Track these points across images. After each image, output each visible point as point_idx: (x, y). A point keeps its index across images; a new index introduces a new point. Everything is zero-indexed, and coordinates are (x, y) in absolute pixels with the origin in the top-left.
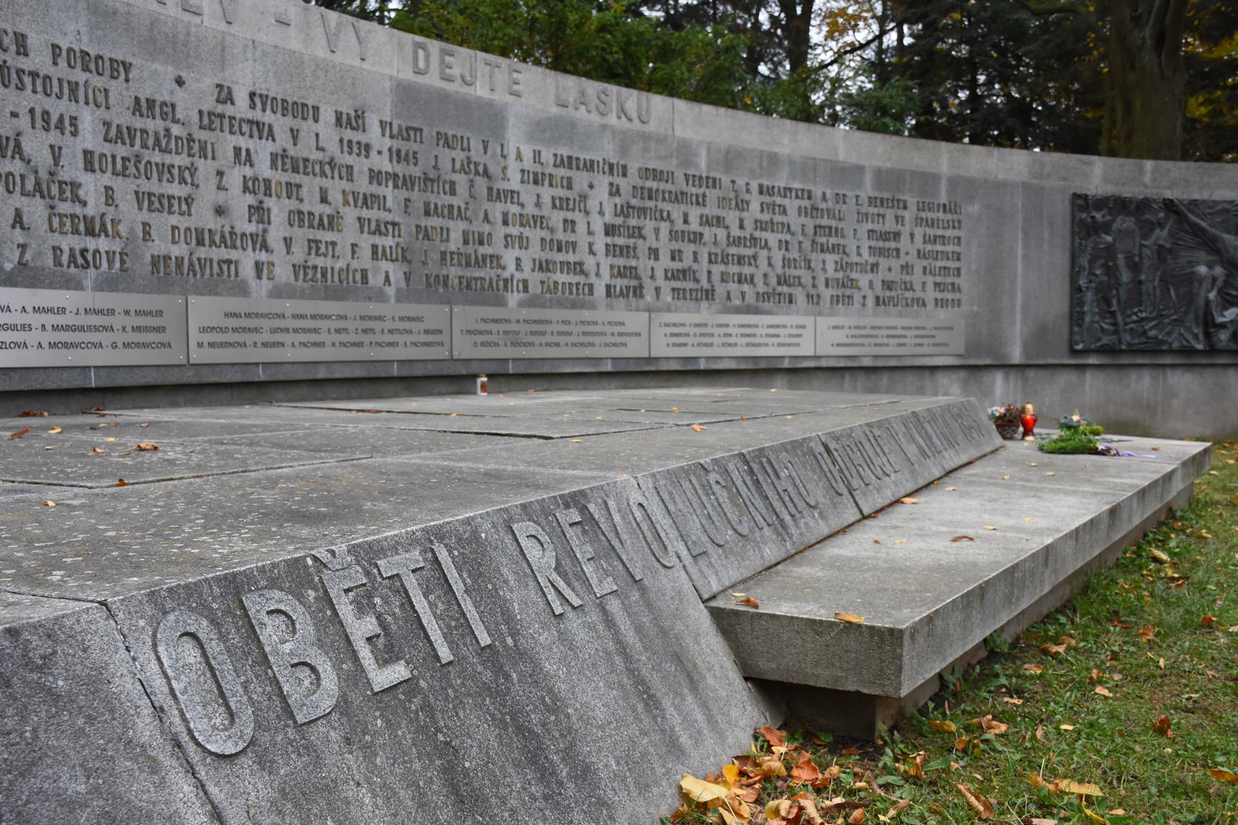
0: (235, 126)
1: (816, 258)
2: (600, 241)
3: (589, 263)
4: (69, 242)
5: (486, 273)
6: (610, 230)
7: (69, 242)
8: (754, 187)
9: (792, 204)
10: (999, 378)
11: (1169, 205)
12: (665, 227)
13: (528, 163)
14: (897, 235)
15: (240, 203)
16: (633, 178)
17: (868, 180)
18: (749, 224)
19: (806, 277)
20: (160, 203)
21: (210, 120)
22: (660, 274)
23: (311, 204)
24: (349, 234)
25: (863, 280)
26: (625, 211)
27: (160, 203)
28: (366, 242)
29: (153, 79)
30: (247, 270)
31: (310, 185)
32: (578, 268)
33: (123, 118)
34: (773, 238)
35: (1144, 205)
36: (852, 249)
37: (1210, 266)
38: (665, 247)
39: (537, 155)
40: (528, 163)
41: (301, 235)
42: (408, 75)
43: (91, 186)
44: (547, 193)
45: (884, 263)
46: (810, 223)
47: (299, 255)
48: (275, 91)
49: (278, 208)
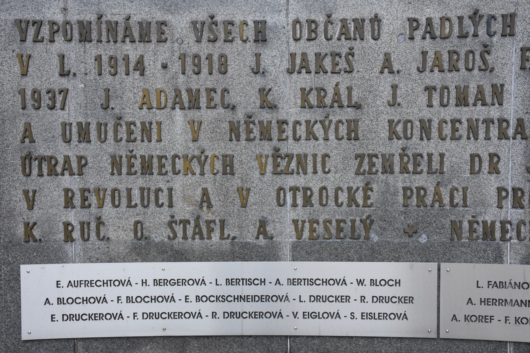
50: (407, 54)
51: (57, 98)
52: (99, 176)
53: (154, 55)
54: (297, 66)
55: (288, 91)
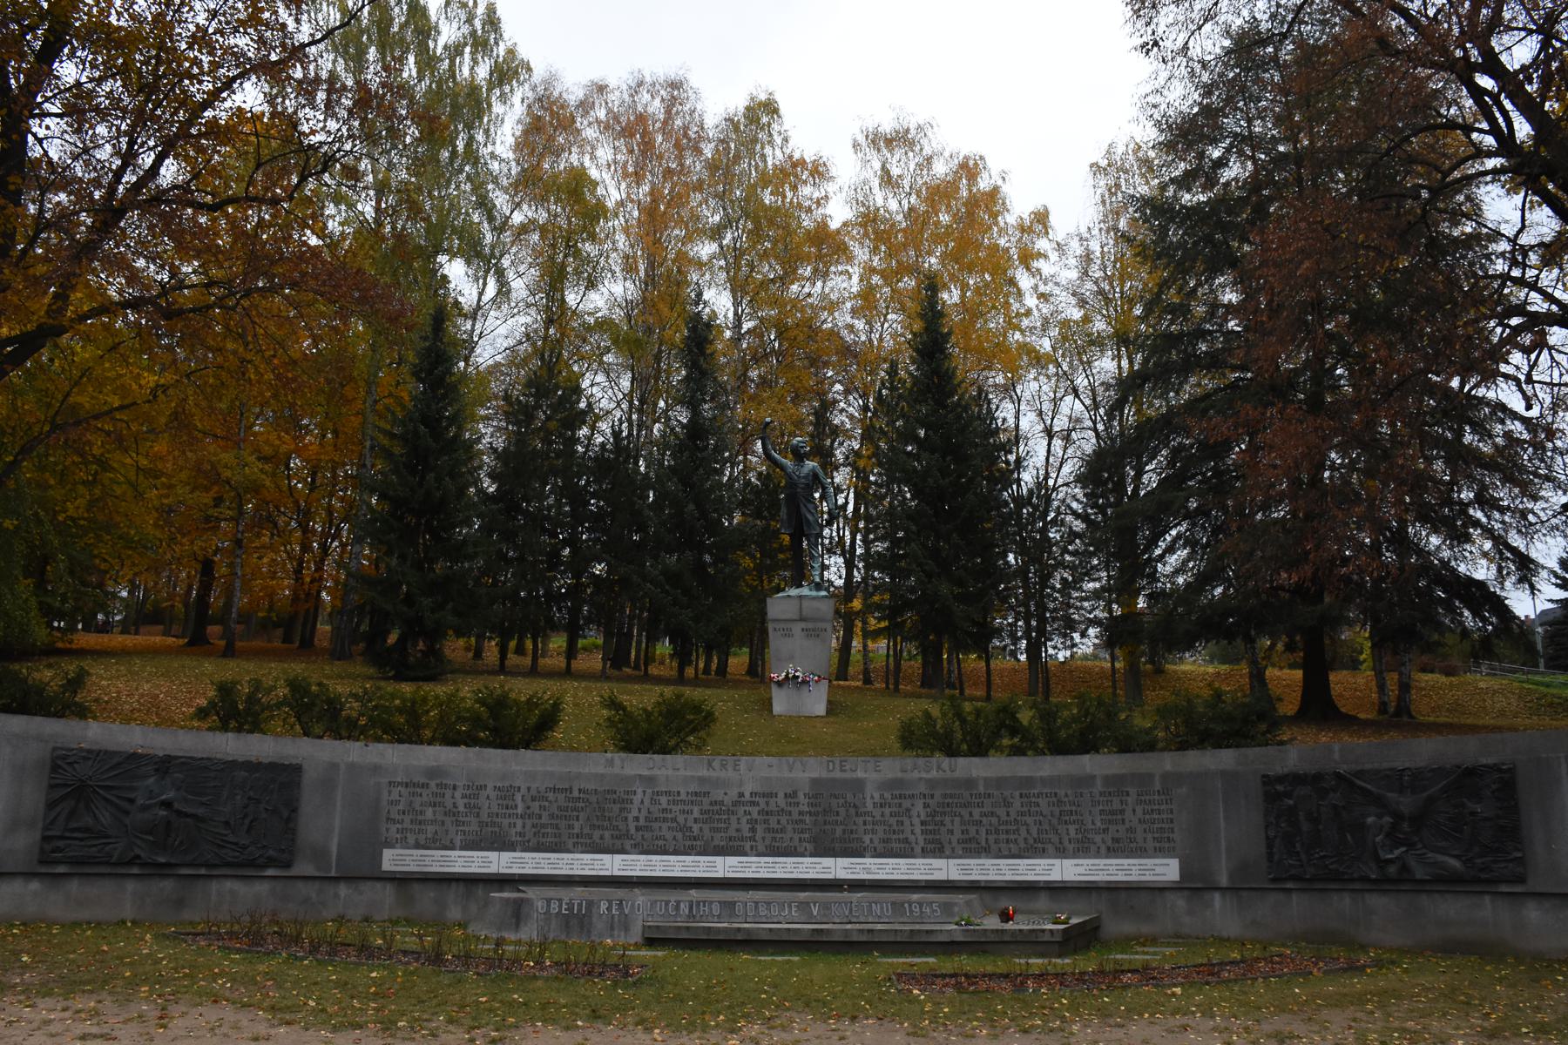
2: (918, 830)
3: (912, 838)
4: (688, 843)
5: (854, 845)
6: (922, 823)
7: (688, 843)
8: (1017, 794)
9: (1043, 802)
10: (1217, 896)
11: (1338, 776)
12: (957, 819)
13: (877, 799)
14: (1122, 812)
15: (745, 827)
16: (938, 798)
17: (1099, 782)
19: (1055, 839)
21: (735, 804)
22: (954, 841)
25: (1098, 839)
26: (933, 814)
28: (796, 837)
29: (718, 794)
30: (747, 848)
31: (773, 820)
32: (906, 840)
33: (706, 807)
34: (1029, 820)
35: (1317, 778)
37: (1380, 816)
38: (957, 828)
39: (882, 796)
40: (877, 799)
42: (824, 774)
43: (696, 828)
44: (887, 811)
45: (1112, 828)
46: (1057, 811)
47: (767, 842)
48: (759, 789)
50: (493, 795)
52: (407, 825)
53: (425, 792)
55: (461, 803)
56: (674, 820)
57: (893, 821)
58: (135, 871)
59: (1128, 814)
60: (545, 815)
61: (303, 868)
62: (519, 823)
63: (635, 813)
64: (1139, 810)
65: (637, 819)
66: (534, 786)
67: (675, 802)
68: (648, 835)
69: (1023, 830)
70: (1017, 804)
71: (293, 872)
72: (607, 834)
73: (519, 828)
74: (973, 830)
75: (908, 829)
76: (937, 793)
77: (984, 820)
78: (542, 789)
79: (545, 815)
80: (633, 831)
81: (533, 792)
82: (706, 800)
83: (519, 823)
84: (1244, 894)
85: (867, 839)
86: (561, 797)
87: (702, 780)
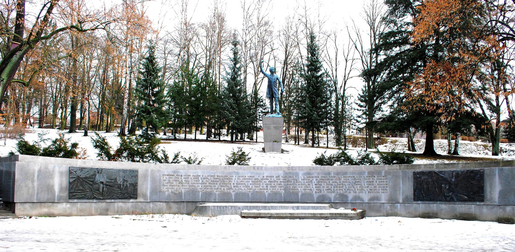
0: (265, 179)
1: (355, 186)
2: (314, 186)
3: (312, 189)
5: (296, 191)
10: (399, 205)
17: (366, 173)
18: (341, 182)
19: (353, 189)
20: (257, 187)
21: (262, 179)
23: (273, 185)
24: (277, 188)
25: (366, 189)
27: (257, 187)
29: (256, 177)
31: (273, 184)
33: (253, 180)
34: (346, 184)
36: (363, 184)
40: (302, 178)
41: (271, 188)
43: (251, 186)
44: (305, 181)
45: (370, 186)
49: (269, 186)
50: (192, 178)
51: (165, 180)
54: (184, 178)
55: (183, 180)
56: (244, 184)
57: (307, 184)
58: (95, 201)
59: (375, 183)
60: (207, 183)
61: (140, 199)
62: (200, 185)
63: (233, 182)
64: (378, 181)
65: (234, 184)
66: (204, 175)
67: (245, 179)
68: (237, 188)
69: (344, 187)
70: (343, 179)
71: (138, 200)
72: (225, 188)
73: (200, 187)
74: (330, 186)
75: (311, 186)
76: (320, 176)
77: (333, 184)
78: (206, 176)
79: (207, 183)
80: (233, 187)
81: (204, 177)
82: (253, 178)
83: (200, 185)
84: (406, 204)
85: (299, 189)
86: (212, 178)
87: (252, 173)
